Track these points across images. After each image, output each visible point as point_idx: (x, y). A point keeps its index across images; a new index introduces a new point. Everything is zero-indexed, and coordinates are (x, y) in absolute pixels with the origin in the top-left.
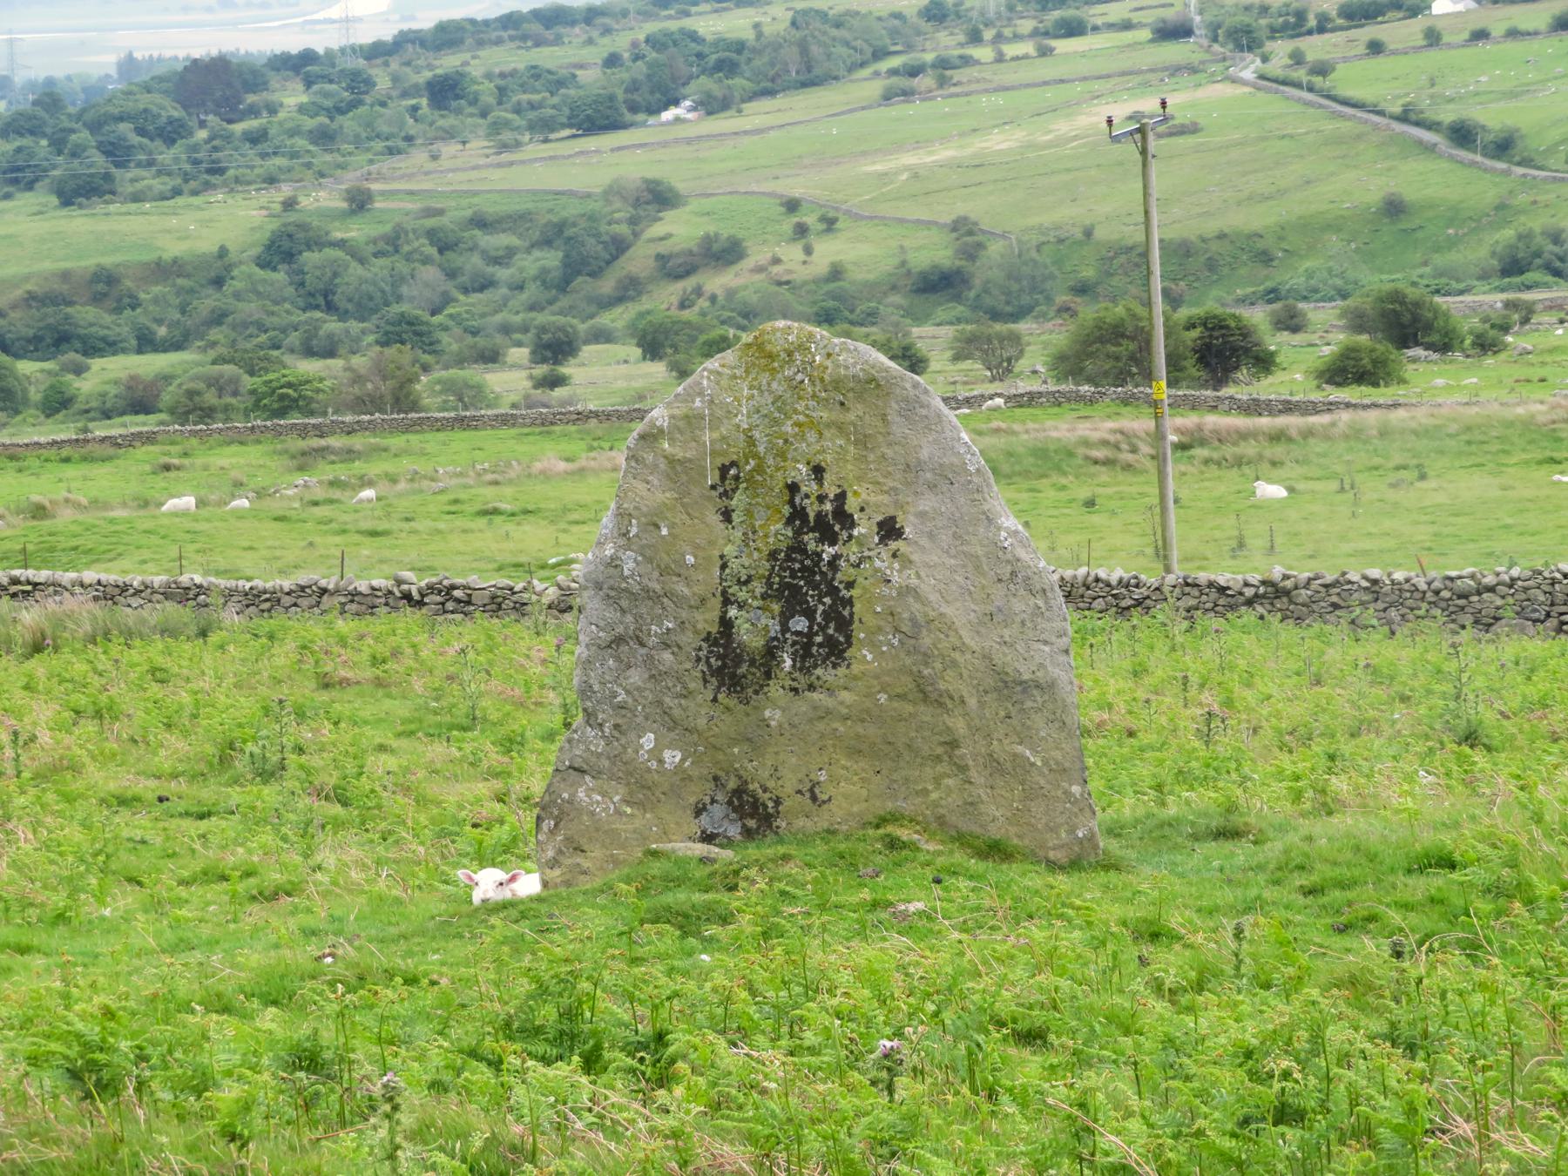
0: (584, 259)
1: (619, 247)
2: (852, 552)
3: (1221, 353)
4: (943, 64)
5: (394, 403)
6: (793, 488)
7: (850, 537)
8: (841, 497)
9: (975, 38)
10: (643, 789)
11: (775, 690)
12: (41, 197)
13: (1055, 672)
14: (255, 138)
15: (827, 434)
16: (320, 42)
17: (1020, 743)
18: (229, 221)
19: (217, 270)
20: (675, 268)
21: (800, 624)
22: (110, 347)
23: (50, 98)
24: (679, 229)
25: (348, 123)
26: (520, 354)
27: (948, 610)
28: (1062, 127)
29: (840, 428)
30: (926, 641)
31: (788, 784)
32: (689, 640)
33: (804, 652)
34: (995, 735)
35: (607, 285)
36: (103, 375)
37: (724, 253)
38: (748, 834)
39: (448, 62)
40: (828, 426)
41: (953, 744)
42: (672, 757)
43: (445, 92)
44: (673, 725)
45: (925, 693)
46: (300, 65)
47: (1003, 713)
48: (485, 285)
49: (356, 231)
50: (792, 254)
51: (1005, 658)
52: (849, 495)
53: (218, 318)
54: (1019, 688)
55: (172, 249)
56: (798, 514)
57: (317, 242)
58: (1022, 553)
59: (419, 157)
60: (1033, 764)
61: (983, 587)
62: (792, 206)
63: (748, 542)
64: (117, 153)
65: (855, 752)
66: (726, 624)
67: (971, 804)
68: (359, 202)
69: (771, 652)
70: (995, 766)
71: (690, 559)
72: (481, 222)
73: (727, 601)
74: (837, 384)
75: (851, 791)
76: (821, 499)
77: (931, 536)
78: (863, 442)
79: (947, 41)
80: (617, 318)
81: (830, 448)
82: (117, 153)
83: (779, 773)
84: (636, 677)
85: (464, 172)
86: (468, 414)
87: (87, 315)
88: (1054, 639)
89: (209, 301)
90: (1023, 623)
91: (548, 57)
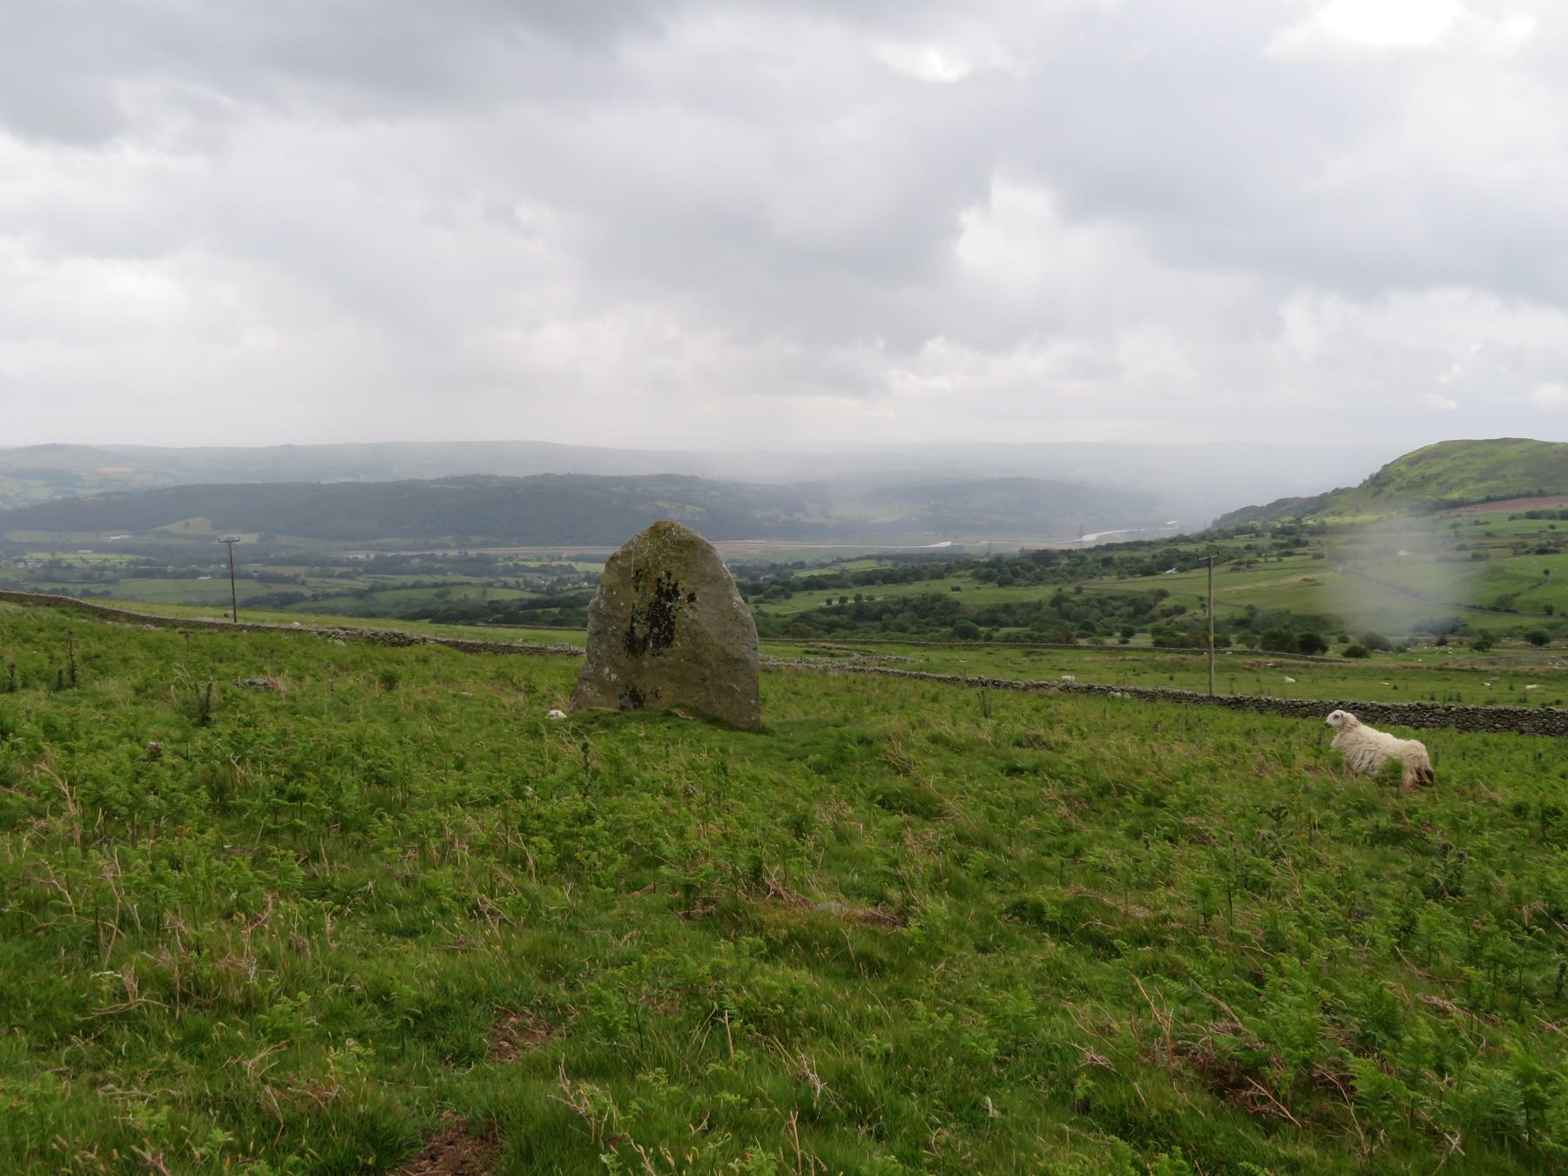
0: (1140, 610)
1: (1150, 607)
2: (677, 605)
3: (1311, 645)
4: (1250, 562)
5: (1067, 642)
9: (1259, 555)
10: (604, 688)
11: (647, 654)
12: (994, 584)
14: (1052, 572)
16: (1073, 548)
18: (1042, 593)
19: (1038, 606)
20: (1166, 613)
21: (656, 630)
22: (1007, 625)
23: (999, 559)
24: (1168, 603)
25: (1079, 569)
26: (1118, 634)
28: (1283, 581)
29: (679, 559)
30: (699, 640)
31: (648, 690)
32: (619, 633)
33: (656, 643)
35: (1147, 617)
36: (1004, 630)
38: (635, 707)
39: (1108, 554)
41: (704, 680)
42: (614, 677)
43: (1107, 562)
44: (615, 666)
45: (696, 659)
46: (1068, 553)
48: (1112, 615)
49: (1076, 598)
50: (1200, 612)
53: (1037, 619)
55: (1026, 600)
56: (660, 590)
57: (1067, 600)
59: (1097, 579)
62: (1201, 599)
63: (639, 599)
64: (1016, 574)
65: (671, 680)
66: (632, 629)
68: (1079, 590)
69: (645, 640)
72: (1112, 598)
74: (679, 543)
75: (668, 693)
78: (686, 565)
79: (1251, 556)
80: (1149, 626)
81: (674, 566)
82: (1016, 574)
83: (646, 685)
84: (604, 646)
85: (1109, 584)
86: (1101, 648)
87: (1002, 616)
89: (1035, 615)
91: (1136, 554)
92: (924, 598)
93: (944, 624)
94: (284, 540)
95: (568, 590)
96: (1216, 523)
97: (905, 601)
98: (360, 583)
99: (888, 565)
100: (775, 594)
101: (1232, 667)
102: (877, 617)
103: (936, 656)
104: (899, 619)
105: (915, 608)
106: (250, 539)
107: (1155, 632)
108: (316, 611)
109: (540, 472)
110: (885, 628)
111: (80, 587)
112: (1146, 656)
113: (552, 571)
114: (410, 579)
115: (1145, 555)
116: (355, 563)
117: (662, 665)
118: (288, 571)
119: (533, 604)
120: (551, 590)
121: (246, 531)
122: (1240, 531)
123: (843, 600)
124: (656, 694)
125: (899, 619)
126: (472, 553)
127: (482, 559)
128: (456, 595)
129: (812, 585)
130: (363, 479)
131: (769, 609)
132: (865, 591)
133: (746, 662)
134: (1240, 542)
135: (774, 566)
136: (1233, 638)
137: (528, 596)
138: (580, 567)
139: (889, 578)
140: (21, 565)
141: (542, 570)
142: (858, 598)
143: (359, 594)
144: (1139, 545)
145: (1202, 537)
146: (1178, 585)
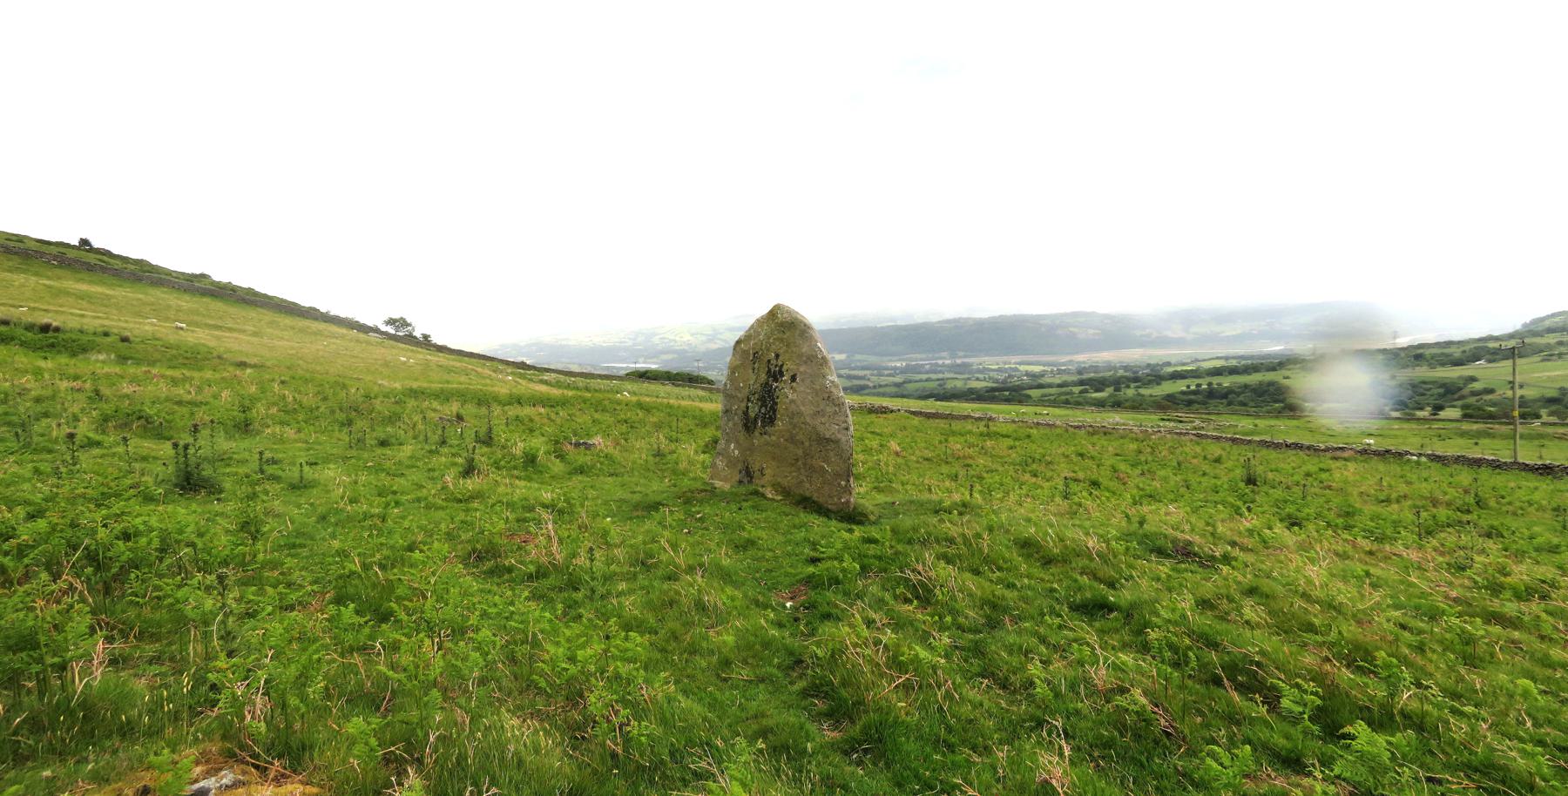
11: (757, 433)
20: (1474, 393)
24: (1477, 386)
37: (1491, 391)
43: (1418, 357)
45: (792, 439)
51: (821, 429)
63: (753, 380)
69: (755, 420)
70: (812, 469)
74: (782, 324)
80: (1459, 403)
91: (1446, 351)
92: (1261, 383)
93: (1276, 401)
94: (858, 357)
95: (1015, 381)
96: (1525, 325)
97: (1246, 386)
98: (898, 379)
99: (1234, 363)
100: (1150, 382)
101: (1541, 436)
102: (1225, 396)
103: (1262, 423)
104: (1241, 398)
105: (1254, 390)
106: (843, 357)
107: (1464, 407)
108: (879, 395)
109: (997, 314)
110: (1229, 404)
112: (1455, 425)
113: (1005, 370)
114: (924, 377)
115: (1456, 352)
116: (895, 368)
117: (768, 444)
118: (861, 373)
119: (993, 390)
120: (1004, 382)
121: (841, 352)
122: (1550, 330)
123: (1198, 385)
124: (761, 470)
125: (1241, 398)
126: (959, 361)
127: (964, 365)
128: (949, 385)
129: (1176, 376)
130: (899, 323)
131: (1143, 391)
132: (1215, 380)
133: (837, 442)
134: (1551, 339)
135: (1149, 365)
136: (1543, 412)
137: (990, 385)
138: (1022, 368)
139: (1233, 371)
141: (999, 370)
142: (1210, 384)
143: (897, 385)
144: (1449, 344)
145: (1511, 336)
146: (1486, 373)
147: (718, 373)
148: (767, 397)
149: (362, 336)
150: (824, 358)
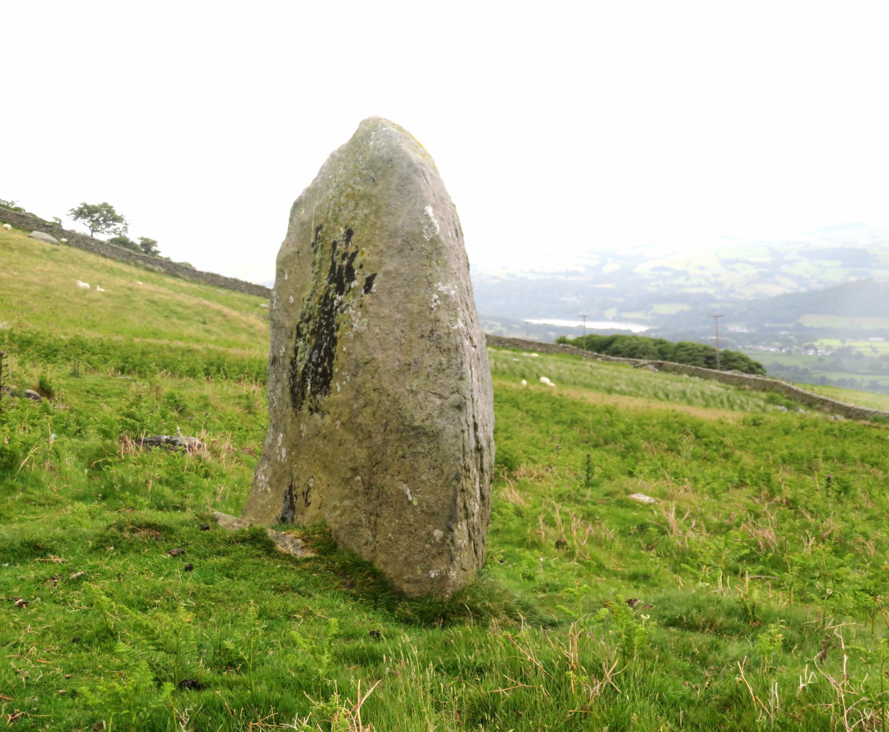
6: (334, 244)
7: (350, 288)
8: (354, 255)
13: (440, 423)
15: (361, 203)
17: (406, 482)
27: (379, 356)
34: (391, 471)
40: (362, 198)
41: (355, 470)
47: (400, 453)
51: (408, 403)
52: (359, 254)
54: (412, 433)
58: (443, 315)
60: (410, 503)
61: (411, 341)
67: (354, 525)
71: (292, 299)
73: (299, 335)
76: (344, 256)
77: (390, 292)
88: (447, 394)
90: (428, 376)
111: (867, 378)
133: (435, 436)
140: (811, 352)
147: (265, 275)
148: (323, 328)
149: (18, 236)
150: (434, 241)
